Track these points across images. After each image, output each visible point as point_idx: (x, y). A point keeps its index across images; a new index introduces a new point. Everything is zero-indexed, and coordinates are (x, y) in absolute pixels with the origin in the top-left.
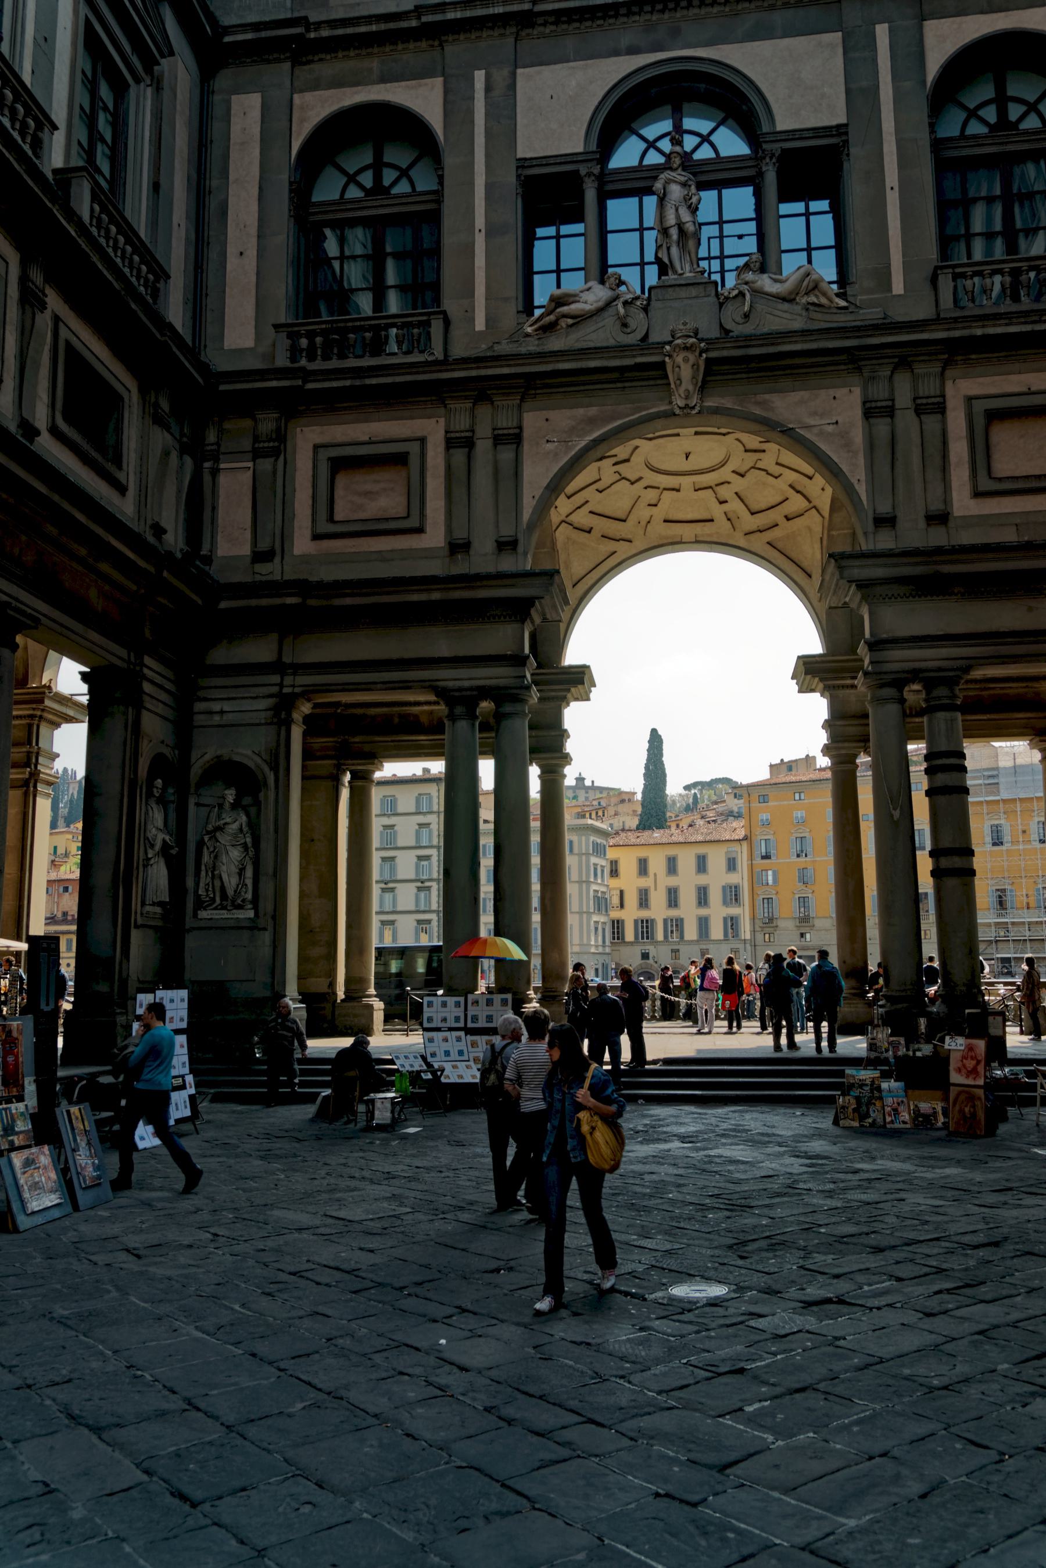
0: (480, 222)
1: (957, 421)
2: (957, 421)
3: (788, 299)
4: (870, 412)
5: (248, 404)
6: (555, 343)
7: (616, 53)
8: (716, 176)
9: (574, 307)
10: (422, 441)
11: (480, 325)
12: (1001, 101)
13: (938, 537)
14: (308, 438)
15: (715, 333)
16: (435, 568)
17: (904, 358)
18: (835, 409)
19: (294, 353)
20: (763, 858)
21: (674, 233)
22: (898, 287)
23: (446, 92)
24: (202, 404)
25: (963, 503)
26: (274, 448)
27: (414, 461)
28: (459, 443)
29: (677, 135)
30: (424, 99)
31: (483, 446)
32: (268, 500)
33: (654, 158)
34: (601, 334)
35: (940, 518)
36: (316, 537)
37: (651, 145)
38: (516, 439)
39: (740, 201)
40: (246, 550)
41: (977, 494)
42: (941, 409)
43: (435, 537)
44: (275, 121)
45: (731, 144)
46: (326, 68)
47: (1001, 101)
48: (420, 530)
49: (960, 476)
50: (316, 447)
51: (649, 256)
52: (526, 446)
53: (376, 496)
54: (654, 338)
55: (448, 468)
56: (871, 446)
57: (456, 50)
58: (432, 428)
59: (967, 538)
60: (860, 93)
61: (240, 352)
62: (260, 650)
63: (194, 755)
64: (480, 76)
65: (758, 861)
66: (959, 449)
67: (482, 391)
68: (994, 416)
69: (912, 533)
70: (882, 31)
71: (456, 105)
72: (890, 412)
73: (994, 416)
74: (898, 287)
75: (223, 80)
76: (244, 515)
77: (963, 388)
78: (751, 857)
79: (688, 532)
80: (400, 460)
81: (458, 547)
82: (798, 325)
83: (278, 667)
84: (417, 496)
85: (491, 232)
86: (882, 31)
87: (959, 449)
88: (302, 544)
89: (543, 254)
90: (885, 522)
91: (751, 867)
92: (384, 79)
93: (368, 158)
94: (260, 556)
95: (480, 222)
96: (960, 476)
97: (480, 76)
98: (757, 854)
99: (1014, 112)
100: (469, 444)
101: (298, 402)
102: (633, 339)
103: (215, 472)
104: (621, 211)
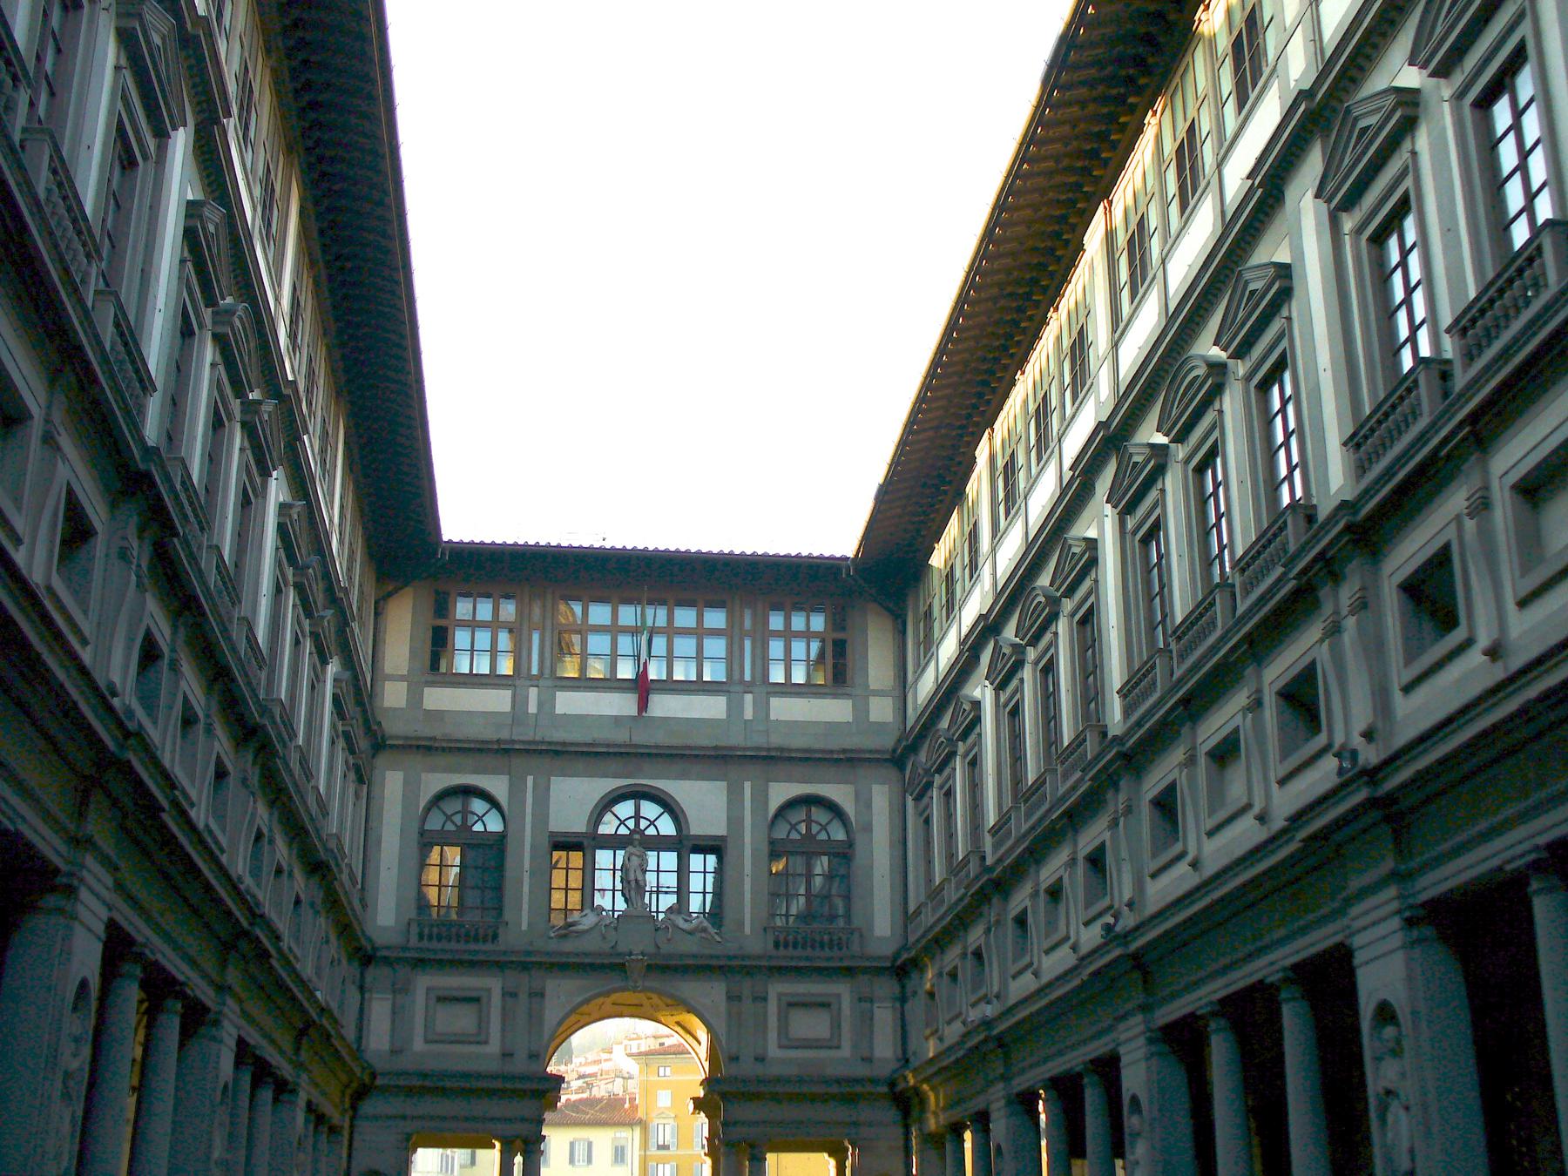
0: (527, 866)
1: (772, 1006)
2: (772, 1006)
3: (691, 933)
4: (730, 998)
5: (386, 961)
6: (568, 946)
7: (606, 776)
8: (660, 843)
9: (580, 927)
10: (489, 990)
11: (524, 927)
12: (809, 821)
13: (760, 1070)
14: (424, 982)
15: (651, 949)
16: (494, 1066)
17: (748, 971)
18: (714, 992)
19: (421, 937)
20: (659, 1147)
21: (633, 884)
22: (747, 930)
23: (511, 785)
24: (365, 957)
25: (773, 1051)
26: (400, 990)
27: (484, 1000)
28: (509, 994)
29: (637, 817)
30: (498, 785)
31: (523, 997)
32: (397, 1014)
33: (623, 831)
34: (590, 944)
35: (760, 1059)
36: (427, 1041)
37: (622, 822)
38: (542, 995)
39: (669, 860)
40: (386, 1047)
41: (780, 1047)
42: (765, 999)
43: (494, 1047)
44: (411, 788)
45: (667, 827)
46: (442, 760)
47: (809, 821)
48: (486, 1042)
49: (772, 1036)
50: (428, 989)
51: (618, 866)
52: (547, 998)
53: (460, 1019)
54: (621, 948)
55: (503, 1008)
56: (729, 1015)
57: (517, 762)
58: (492, 984)
59: (775, 1070)
60: (735, 821)
61: (385, 929)
62: (395, 1105)
63: (354, 1164)
64: (530, 779)
65: (653, 1151)
66: (773, 1021)
67: (525, 967)
68: (791, 1005)
69: (747, 1068)
70: (747, 785)
71: (516, 790)
72: (739, 998)
73: (791, 1005)
74: (747, 930)
75: (381, 761)
76: (387, 1026)
77: (778, 989)
78: (645, 1145)
79: (626, 1010)
80: (478, 1000)
81: (507, 1055)
82: (694, 949)
83: (404, 1118)
84: (482, 1022)
85: (532, 874)
86: (747, 785)
87: (773, 1021)
88: (418, 1045)
89: (558, 878)
90: (734, 1059)
91: (644, 1161)
92: (476, 771)
93: (459, 807)
94: (395, 1052)
95: (527, 866)
96: (772, 1036)
97: (530, 779)
98: (652, 1143)
99: (815, 829)
100: (514, 995)
101: (420, 963)
102: (606, 947)
103: (370, 1000)
104: (604, 858)
